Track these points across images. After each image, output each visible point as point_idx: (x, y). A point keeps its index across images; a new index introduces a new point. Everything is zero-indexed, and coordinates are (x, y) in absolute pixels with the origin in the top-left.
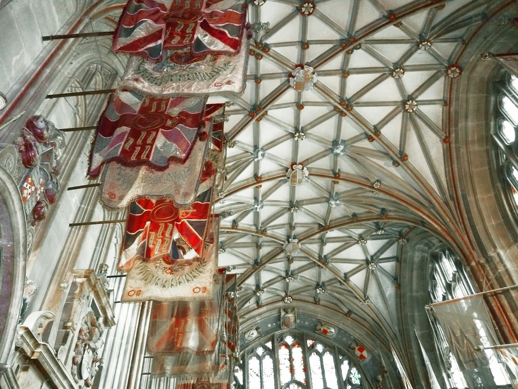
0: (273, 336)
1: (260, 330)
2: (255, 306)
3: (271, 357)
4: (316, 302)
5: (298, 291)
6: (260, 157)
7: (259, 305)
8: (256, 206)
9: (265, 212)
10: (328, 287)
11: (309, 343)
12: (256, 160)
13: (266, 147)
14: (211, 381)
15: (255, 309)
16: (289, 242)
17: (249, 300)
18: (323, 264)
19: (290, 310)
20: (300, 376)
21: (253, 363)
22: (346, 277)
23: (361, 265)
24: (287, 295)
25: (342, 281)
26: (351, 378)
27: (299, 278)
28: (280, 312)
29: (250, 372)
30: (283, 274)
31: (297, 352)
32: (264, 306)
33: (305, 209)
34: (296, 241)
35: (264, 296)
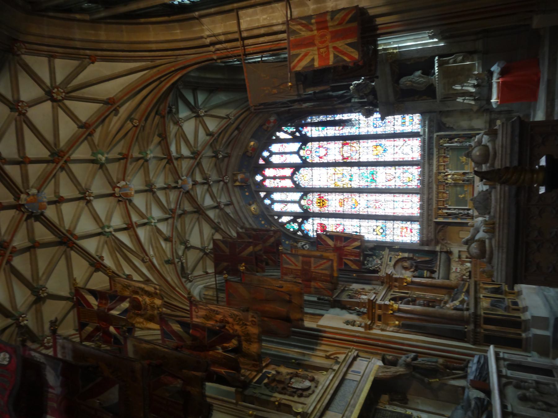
0: (256, 191)
1: (251, 202)
2: (231, 207)
4: (228, 156)
5: (219, 172)
6: (111, 229)
8: (153, 224)
9: (156, 213)
10: (218, 148)
11: (261, 162)
12: (113, 233)
13: (100, 224)
14: (300, 268)
15: (234, 207)
16: (181, 188)
18: (199, 155)
19: (235, 178)
20: (288, 172)
21: (277, 207)
22: (209, 134)
23: (200, 122)
24: (223, 181)
27: (209, 173)
28: (237, 186)
29: (284, 210)
30: (206, 187)
31: (269, 172)
33: (153, 177)
34: (180, 182)
35: (224, 200)
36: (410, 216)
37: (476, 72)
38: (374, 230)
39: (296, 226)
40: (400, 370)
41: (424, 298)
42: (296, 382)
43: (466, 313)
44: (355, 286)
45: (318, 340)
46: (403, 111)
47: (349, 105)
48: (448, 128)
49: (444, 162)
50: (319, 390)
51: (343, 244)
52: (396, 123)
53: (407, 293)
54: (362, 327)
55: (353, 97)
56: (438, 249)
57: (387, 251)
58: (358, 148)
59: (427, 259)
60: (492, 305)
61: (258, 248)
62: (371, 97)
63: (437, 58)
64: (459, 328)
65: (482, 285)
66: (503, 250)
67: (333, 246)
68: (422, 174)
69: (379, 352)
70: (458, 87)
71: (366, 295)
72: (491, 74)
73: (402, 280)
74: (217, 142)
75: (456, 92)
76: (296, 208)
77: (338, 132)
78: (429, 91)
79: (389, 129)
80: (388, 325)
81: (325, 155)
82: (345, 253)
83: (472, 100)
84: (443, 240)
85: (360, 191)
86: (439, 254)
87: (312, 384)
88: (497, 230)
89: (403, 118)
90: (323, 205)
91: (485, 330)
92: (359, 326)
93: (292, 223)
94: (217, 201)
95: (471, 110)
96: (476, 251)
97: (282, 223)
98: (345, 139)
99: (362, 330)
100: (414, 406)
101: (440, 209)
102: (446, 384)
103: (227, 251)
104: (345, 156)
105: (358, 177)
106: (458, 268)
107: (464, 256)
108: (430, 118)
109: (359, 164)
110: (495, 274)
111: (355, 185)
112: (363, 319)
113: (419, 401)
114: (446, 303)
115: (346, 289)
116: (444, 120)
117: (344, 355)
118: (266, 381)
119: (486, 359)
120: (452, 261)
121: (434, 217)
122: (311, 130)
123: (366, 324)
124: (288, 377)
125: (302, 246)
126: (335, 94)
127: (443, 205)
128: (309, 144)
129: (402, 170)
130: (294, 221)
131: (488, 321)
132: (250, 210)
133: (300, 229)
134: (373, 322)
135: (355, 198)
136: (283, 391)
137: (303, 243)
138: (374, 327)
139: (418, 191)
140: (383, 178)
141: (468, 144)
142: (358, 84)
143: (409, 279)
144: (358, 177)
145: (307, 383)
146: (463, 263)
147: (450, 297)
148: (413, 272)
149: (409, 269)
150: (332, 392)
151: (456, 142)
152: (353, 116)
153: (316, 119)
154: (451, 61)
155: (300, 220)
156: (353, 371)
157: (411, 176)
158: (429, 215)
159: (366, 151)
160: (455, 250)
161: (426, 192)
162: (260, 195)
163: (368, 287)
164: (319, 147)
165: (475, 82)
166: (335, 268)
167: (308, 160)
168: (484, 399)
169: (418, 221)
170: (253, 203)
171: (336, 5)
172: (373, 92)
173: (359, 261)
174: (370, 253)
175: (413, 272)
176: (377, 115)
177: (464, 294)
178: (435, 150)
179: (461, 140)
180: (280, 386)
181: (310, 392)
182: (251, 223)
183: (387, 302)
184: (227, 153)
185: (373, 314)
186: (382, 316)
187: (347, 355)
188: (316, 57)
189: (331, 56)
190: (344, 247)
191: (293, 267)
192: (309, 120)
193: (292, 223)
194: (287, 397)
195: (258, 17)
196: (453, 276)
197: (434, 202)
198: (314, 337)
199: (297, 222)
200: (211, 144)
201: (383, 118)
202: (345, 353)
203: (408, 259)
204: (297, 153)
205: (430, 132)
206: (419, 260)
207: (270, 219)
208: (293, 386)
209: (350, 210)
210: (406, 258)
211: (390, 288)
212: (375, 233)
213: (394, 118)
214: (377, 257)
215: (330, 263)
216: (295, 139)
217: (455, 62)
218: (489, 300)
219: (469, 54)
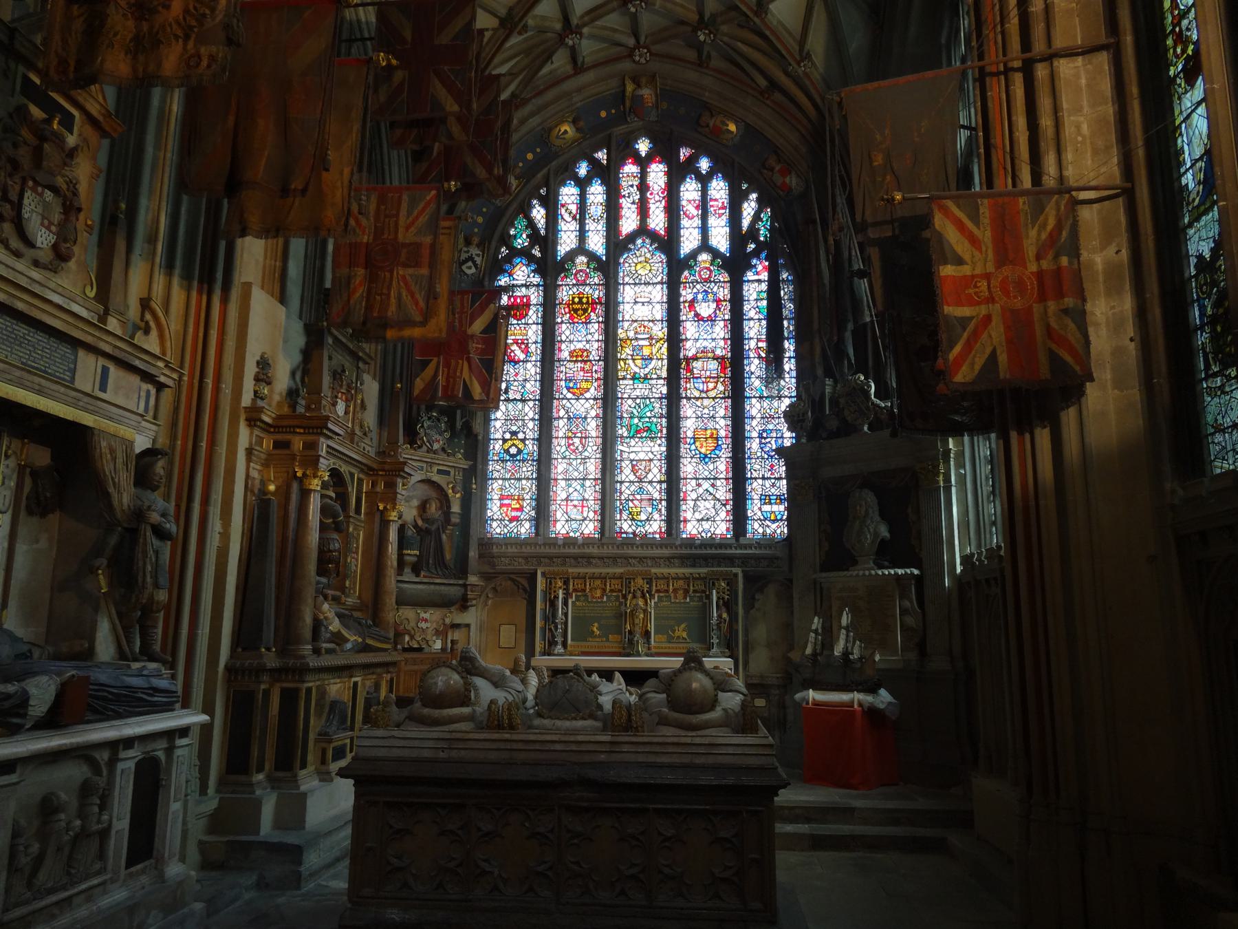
0: (610, 136)
1: (582, 124)
2: (569, 69)
3: (604, 182)
4: (701, 63)
7: (578, 67)
10: (724, 28)
11: (684, 153)
14: (400, 236)
15: (568, 77)
17: (549, 57)
19: (643, 80)
20: (658, 221)
21: (568, 194)
24: (638, 45)
25: (749, 13)
26: (759, 230)
28: (624, 85)
31: (657, 175)
32: (589, 68)
35: (588, 48)
36: (549, 516)
37: (877, 658)
38: (514, 433)
39: (521, 241)
40: (124, 495)
41: (347, 548)
42: (46, 206)
44: (371, 388)
45: (201, 282)
46: (794, 499)
47: (820, 372)
48: (753, 598)
49: (675, 590)
51: (475, 358)
52: (768, 483)
53: (358, 511)
55: (836, 382)
56: (473, 579)
57: (465, 464)
58: (712, 394)
59: (448, 556)
60: (334, 704)
61: (456, 129)
62: (833, 424)
63: (916, 572)
64: (269, 633)
65: (387, 677)
66: (443, 749)
67: (469, 332)
68: (646, 542)
70: (845, 620)
71: (346, 413)
72: (873, 690)
73: (391, 496)
74: (740, 26)
75: (834, 614)
76: (567, 241)
77: (753, 344)
78: (839, 557)
79: (755, 468)
80: (266, 464)
81: (697, 315)
82: (453, 362)
83: (814, 650)
84: (494, 589)
85: (609, 400)
86: (461, 582)
87: (46, 256)
88: (496, 736)
89: (780, 499)
90: (576, 311)
91: (267, 693)
92: (256, 392)
93: (529, 232)
94: (585, 25)
95: (791, 648)
96: (440, 683)
97: (531, 207)
98: (734, 364)
99: (247, 399)
100: (22, 531)
101: (566, 583)
102: (96, 610)
103: (444, 39)
104: (697, 365)
105: (641, 393)
106: (428, 625)
107: (457, 635)
108: (777, 558)
109: (673, 399)
110: (380, 733)
111: (625, 388)
112: (279, 404)
113: (43, 544)
114: (336, 599)
115: (361, 365)
116: (771, 590)
117: (156, 350)
118: (36, 112)
119: (166, 708)
120: (445, 610)
121: (547, 569)
122: (759, 281)
123: (261, 410)
124: (60, 181)
125: (471, 259)
126: (848, 335)
127: (575, 590)
128: (724, 277)
129: (656, 495)
130: (535, 237)
131: (290, 698)
132: (562, 122)
133: (515, 253)
134: (267, 428)
135: (592, 390)
137: (478, 260)
138: (257, 432)
139: (607, 535)
140: (642, 453)
141: (715, 641)
142: (867, 393)
143: (393, 515)
144: (641, 393)
145: (44, 239)
146: (441, 633)
147: (354, 608)
148: (416, 526)
149: (421, 516)
150: (20, 306)
151: (720, 616)
152: (789, 382)
153: (785, 292)
154: (907, 604)
155: (536, 252)
156: (105, 371)
157: (643, 517)
158: (551, 558)
159: (704, 413)
160: (470, 617)
161: (606, 551)
162: (601, 149)
163: (370, 418)
164: (718, 301)
165: (856, 654)
166: (407, 333)
167: (686, 273)
168: (24, 716)
169: (537, 534)
170: (578, 130)
171: (1097, 325)
172: (847, 429)
173: (434, 397)
174: (459, 425)
175: (416, 526)
176: (788, 439)
177: (360, 640)
178: (703, 570)
179: (725, 626)
181: (15, 243)
182: (525, 123)
183: (324, 464)
184: (709, 56)
185: (291, 430)
186: (287, 452)
187: (159, 358)
188: (966, 270)
189: (965, 311)
190: (469, 360)
191: (402, 221)
192: (785, 275)
193: (529, 232)
195: (1086, 110)
196: (408, 613)
197: (582, 570)
198: (207, 267)
199: (532, 246)
200: (736, 8)
201: (781, 451)
203: (447, 514)
204: (705, 246)
205: (744, 560)
206: (444, 537)
207: (540, 175)
208: (28, 194)
209: (562, 376)
210: (449, 507)
211: (368, 470)
212: (508, 436)
213: (780, 479)
214: (450, 440)
215: (418, 318)
216: (738, 237)
217: (904, 612)
218: (346, 697)
219: (920, 644)
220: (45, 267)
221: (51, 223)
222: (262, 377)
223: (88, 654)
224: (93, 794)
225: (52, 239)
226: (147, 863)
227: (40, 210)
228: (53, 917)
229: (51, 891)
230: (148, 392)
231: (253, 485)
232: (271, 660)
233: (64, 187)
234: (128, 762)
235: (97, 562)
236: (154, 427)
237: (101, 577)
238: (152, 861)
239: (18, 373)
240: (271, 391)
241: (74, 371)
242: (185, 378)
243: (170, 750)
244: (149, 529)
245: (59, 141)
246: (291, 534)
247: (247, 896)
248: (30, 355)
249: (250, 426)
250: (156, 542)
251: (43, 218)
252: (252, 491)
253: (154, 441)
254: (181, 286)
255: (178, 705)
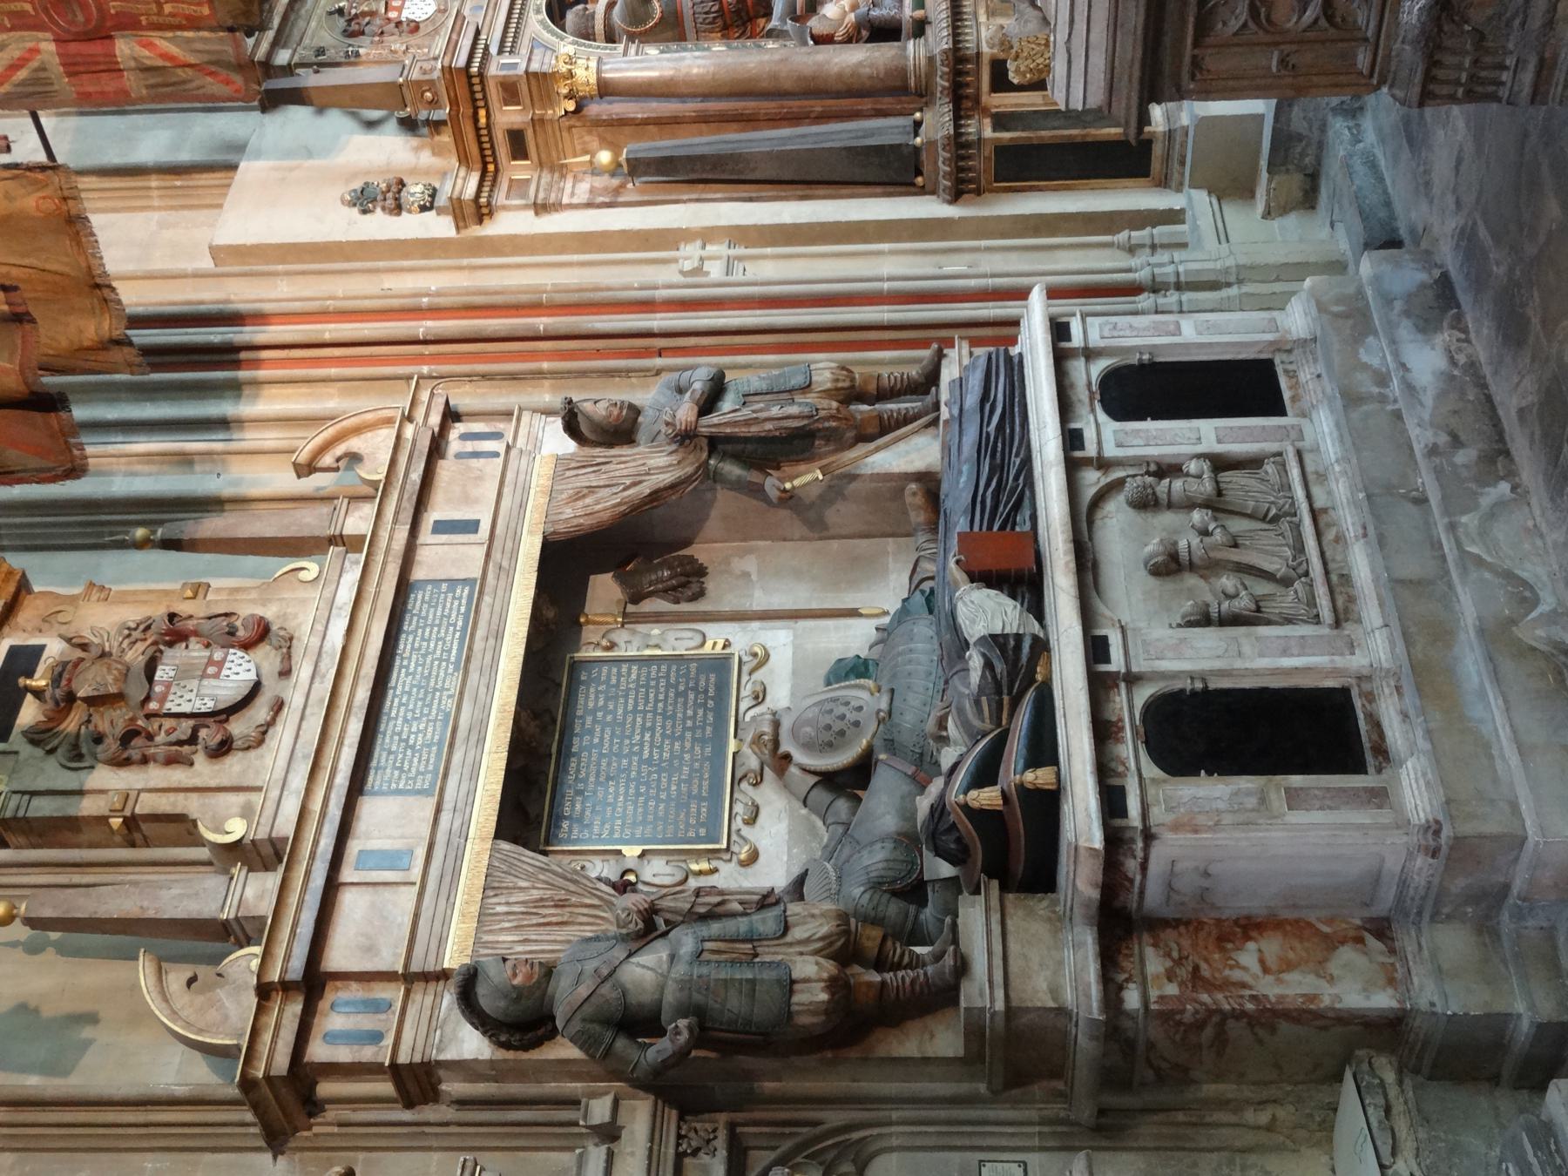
40: (652, 466)
42: (184, 673)
43: (914, 51)
45: (237, 365)
50: (304, 691)
54: (440, 212)
69: (545, 365)
80: (562, 170)
87: (266, 658)
92: (423, 209)
99: (440, 226)
100: (728, 603)
102: (853, 477)
110: (1059, 67)
112: (437, 151)
113: (750, 564)
117: (386, 436)
119: (1015, 370)
124: (136, 656)
134: (489, 175)
136: (130, 748)
138: (500, 198)
145: (239, 670)
150: (363, 694)
156: (441, 527)
168: (1019, 638)
180: (112, 722)
181: (260, 712)
185: (483, 137)
186: (529, 134)
194: (157, 775)
202: (389, 421)
220: (288, 657)
221: (210, 662)
222: (390, 202)
223: (929, 483)
224: (1155, 486)
225: (236, 655)
226: (1279, 370)
227: (194, 684)
228: (1339, 539)
229: (1299, 548)
230: (465, 437)
231: (606, 190)
232: (937, 122)
233: (140, 646)
234: (1107, 434)
235: (773, 494)
236: (526, 417)
237: (797, 482)
238: (1277, 361)
239: (474, 676)
240: (414, 171)
241: (453, 583)
242: (425, 369)
243: (1089, 354)
244: (706, 420)
245: (61, 672)
246: (690, 107)
247: (1370, 137)
248: (441, 660)
249: (491, 214)
250: (727, 404)
251: (204, 676)
252: (617, 191)
253: (548, 412)
254: (255, 397)
255: (1014, 351)
